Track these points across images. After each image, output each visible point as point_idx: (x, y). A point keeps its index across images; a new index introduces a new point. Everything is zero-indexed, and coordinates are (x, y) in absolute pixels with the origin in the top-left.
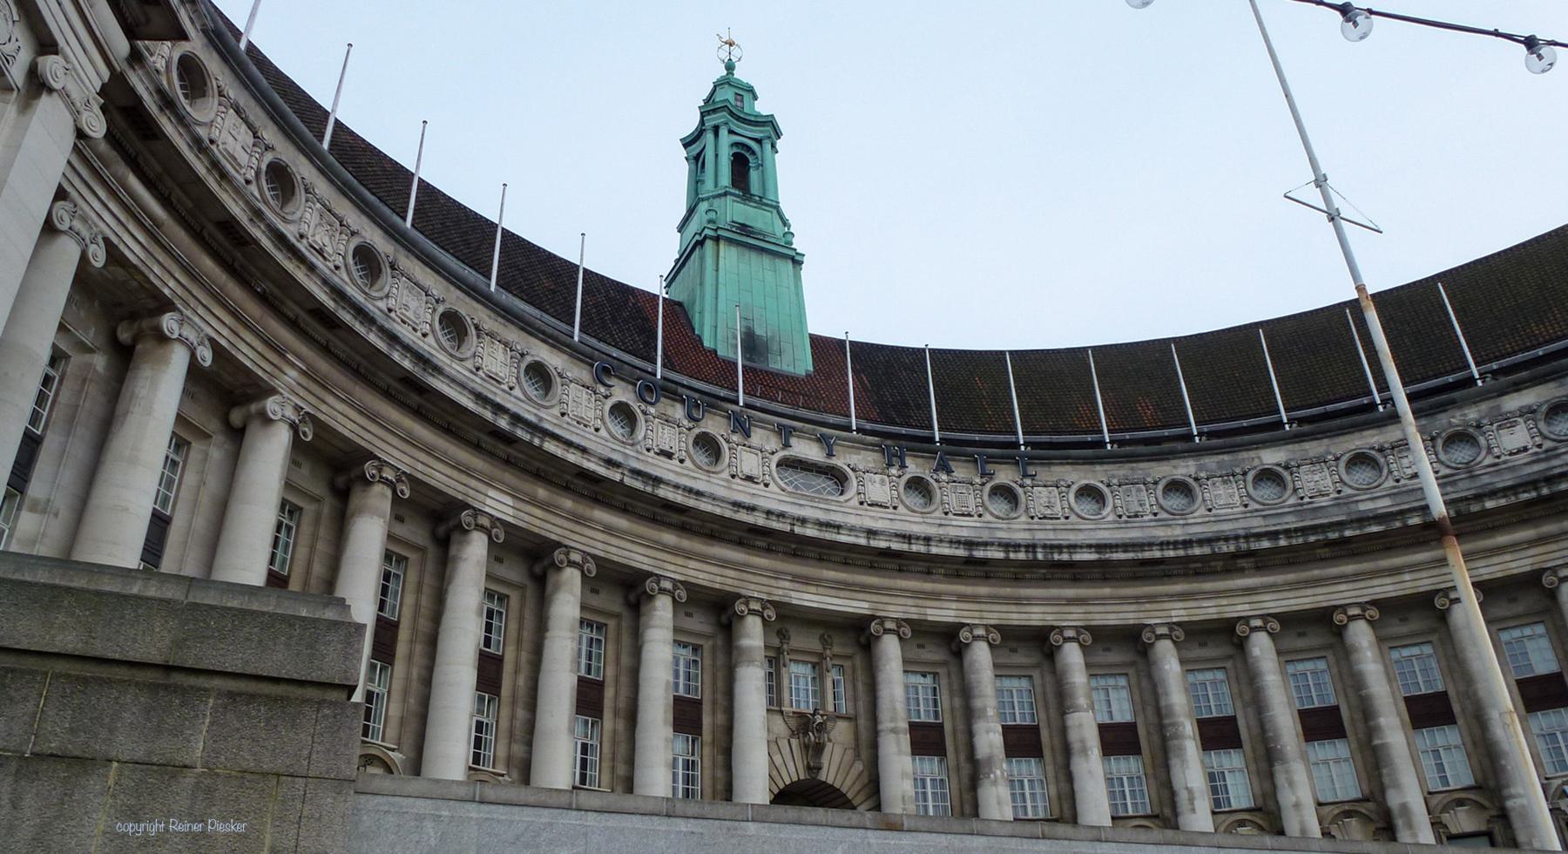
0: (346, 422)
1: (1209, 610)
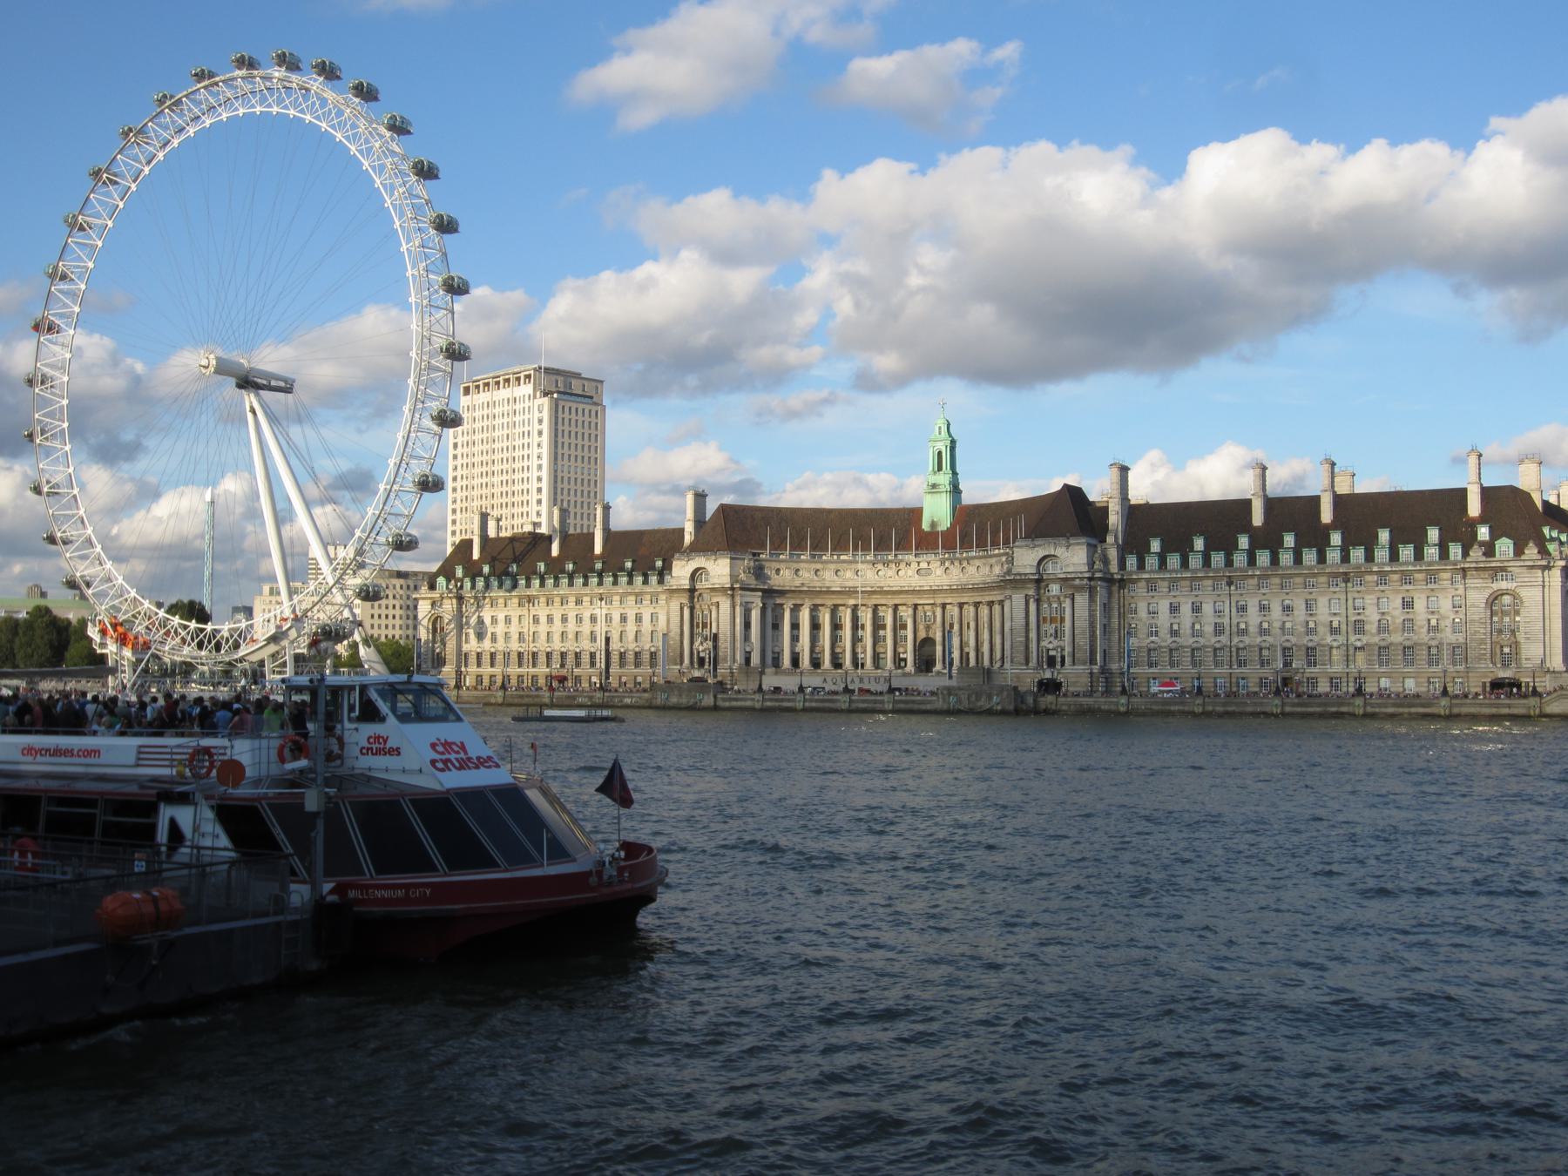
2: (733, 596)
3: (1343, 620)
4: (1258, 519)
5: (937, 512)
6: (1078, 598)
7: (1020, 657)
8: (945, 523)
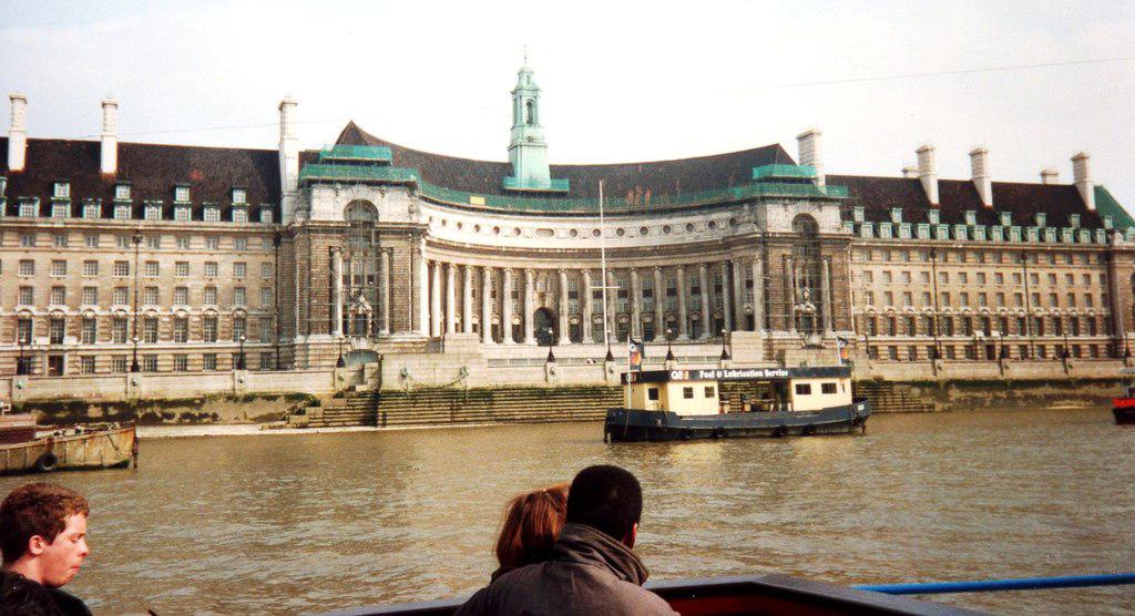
3: (1023, 292)
4: (934, 198)
5: (533, 170)
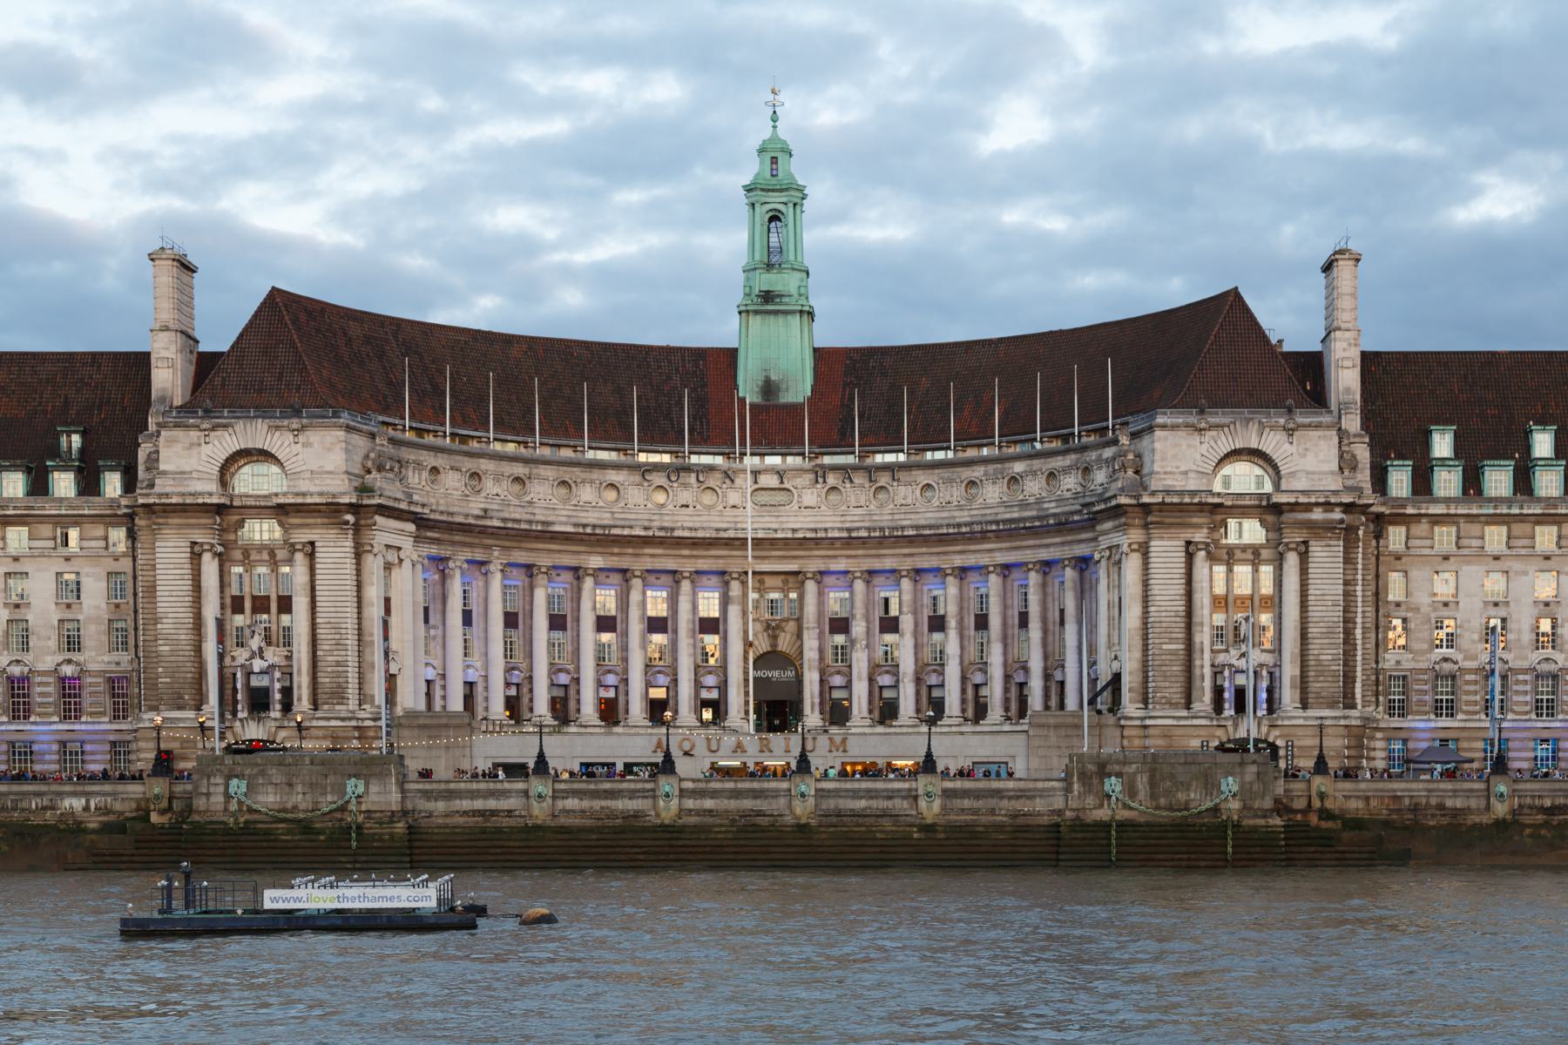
0: (521, 557)
1: (971, 560)
2: (357, 528)
5: (780, 359)
6: (1318, 551)
7: (1175, 691)
8: (800, 387)
